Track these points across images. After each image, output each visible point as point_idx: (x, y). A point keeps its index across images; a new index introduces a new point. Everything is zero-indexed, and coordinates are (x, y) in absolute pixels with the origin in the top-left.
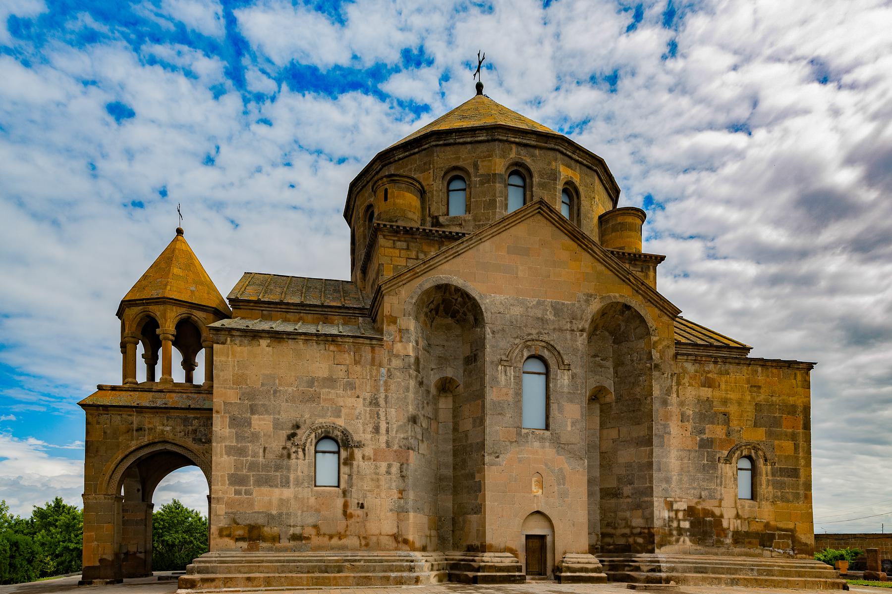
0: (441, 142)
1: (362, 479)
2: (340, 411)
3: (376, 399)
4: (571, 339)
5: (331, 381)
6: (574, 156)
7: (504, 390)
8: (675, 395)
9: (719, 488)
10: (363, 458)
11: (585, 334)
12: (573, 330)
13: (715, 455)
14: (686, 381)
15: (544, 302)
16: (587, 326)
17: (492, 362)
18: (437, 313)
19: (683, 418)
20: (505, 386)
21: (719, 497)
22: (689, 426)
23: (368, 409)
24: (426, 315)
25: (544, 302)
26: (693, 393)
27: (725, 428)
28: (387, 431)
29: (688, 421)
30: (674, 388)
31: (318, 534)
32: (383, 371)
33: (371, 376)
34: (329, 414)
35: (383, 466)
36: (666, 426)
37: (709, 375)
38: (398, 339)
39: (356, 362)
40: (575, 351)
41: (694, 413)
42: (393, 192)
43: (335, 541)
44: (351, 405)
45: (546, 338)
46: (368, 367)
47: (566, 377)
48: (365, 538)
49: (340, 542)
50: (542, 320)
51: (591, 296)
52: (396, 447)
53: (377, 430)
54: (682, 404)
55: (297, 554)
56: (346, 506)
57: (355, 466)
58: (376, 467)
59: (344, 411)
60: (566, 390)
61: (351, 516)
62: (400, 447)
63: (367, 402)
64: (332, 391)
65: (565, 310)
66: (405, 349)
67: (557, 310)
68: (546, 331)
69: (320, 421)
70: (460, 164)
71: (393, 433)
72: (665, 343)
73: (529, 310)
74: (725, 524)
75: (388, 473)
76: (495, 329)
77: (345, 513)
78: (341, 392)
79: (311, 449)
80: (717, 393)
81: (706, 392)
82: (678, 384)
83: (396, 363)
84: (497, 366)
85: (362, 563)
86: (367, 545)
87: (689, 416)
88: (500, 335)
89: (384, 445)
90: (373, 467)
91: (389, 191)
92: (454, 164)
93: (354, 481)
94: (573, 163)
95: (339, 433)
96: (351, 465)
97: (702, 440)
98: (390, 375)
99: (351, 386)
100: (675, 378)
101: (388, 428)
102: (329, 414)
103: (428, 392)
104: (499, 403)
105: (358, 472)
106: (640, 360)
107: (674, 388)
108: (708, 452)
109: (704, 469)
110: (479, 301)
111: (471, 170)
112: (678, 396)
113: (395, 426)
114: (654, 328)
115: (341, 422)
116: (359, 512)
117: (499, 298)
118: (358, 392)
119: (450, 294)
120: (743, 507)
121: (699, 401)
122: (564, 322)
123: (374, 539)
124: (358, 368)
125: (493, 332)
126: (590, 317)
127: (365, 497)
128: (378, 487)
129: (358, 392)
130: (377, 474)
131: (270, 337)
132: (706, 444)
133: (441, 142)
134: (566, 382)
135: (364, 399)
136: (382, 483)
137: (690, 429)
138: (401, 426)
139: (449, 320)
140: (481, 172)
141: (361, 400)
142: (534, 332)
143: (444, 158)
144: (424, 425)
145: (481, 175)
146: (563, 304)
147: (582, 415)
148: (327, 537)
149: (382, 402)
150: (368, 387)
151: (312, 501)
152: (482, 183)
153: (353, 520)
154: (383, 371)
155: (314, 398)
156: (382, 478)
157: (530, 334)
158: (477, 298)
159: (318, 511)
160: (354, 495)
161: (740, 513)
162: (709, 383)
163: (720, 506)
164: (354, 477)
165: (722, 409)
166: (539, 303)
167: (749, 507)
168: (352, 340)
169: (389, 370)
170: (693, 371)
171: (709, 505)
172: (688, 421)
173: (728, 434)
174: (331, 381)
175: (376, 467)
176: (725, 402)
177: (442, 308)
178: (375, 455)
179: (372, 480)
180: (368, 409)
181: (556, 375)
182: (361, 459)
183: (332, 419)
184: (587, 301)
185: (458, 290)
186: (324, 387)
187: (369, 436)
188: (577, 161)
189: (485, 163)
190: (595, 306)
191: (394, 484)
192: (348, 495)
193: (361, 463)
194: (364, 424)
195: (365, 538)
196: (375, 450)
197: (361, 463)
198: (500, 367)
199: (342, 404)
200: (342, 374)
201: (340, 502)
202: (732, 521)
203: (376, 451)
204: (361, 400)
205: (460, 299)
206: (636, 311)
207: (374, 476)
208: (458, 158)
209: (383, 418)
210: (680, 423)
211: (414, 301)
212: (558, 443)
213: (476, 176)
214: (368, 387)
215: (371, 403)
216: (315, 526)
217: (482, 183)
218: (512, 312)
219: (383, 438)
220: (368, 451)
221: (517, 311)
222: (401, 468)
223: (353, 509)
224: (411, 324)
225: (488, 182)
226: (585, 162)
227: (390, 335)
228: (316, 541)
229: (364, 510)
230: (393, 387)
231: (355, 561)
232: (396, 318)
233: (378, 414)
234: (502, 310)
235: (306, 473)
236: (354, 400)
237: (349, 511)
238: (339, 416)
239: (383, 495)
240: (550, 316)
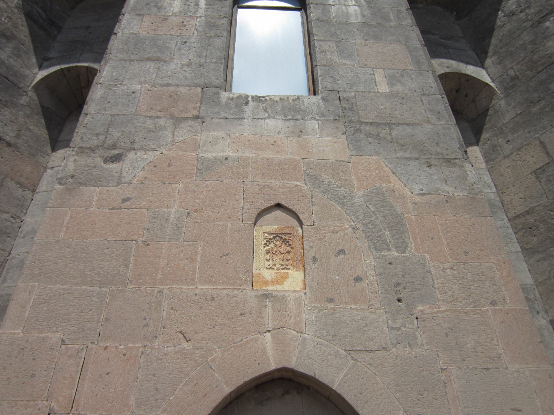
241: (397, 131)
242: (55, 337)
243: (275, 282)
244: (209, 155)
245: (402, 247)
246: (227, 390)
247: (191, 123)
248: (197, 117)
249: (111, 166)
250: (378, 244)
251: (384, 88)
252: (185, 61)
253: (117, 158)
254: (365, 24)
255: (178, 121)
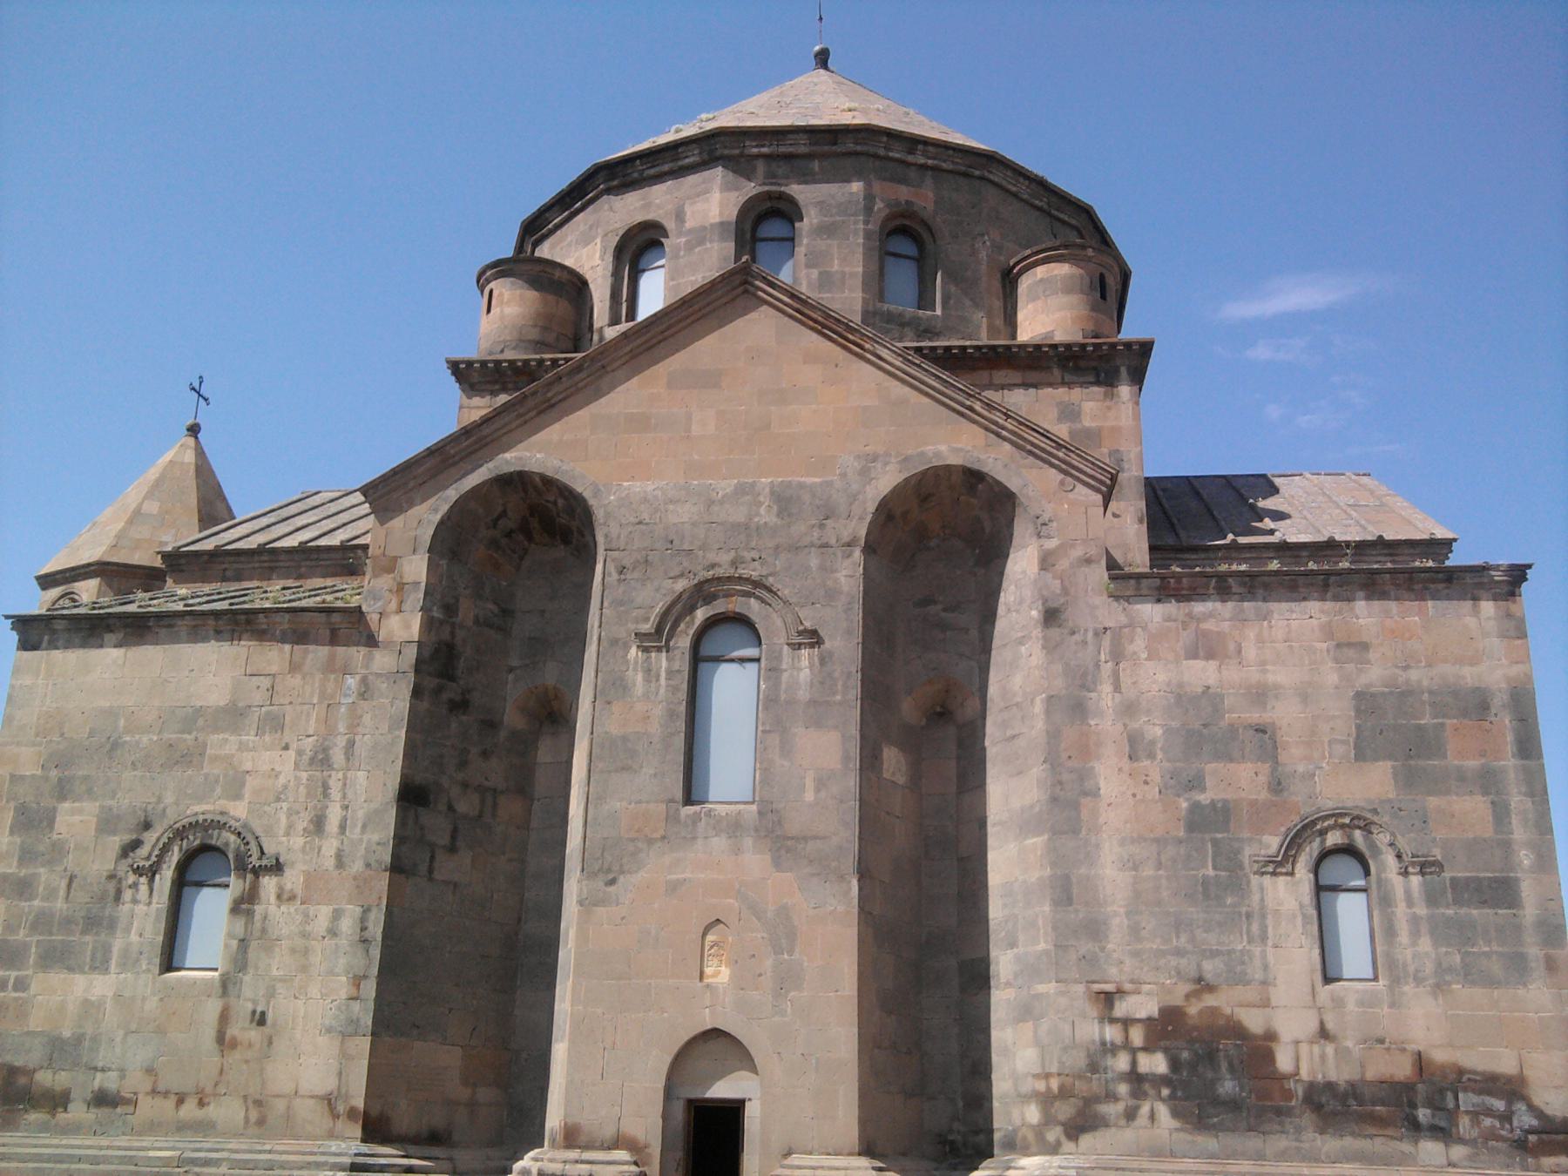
0: (615, 183)
1: (269, 950)
2: (243, 784)
3: (325, 750)
4: (822, 568)
5: (233, 716)
6: (910, 158)
7: (640, 707)
8: (1106, 688)
9: (1257, 950)
10: (279, 897)
11: (857, 554)
12: (826, 546)
13: (1238, 852)
14: (1138, 645)
15: (753, 485)
16: (863, 533)
17: (614, 642)
18: (530, 538)
19: (1136, 748)
20: (646, 696)
21: (1259, 976)
22: (1155, 770)
23: (304, 775)
24: (494, 544)
25: (753, 485)
26: (1162, 677)
27: (1265, 768)
28: (343, 827)
29: (1151, 756)
30: (1107, 668)
31: (154, 1092)
32: (351, 682)
33: (323, 695)
34: (219, 790)
35: (324, 912)
36: (1084, 775)
37: (1204, 626)
38: (393, 605)
39: (294, 667)
40: (831, 595)
41: (1168, 731)
42: (501, 295)
43: (189, 1110)
44: (266, 767)
45: (753, 571)
46: (319, 676)
47: (805, 663)
48: (259, 1103)
49: (200, 1114)
50: (746, 529)
51: (875, 459)
52: (357, 866)
53: (319, 824)
54: (1129, 709)
55: (104, 1142)
56: (224, 1018)
57: (257, 917)
58: (307, 918)
59: (251, 783)
60: (803, 694)
61: (234, 1044)
62: (368, 865)
63: (306, 758)
64: (232, 738)
65: (807, 498)
66: (408, 627)
67: (785, 501)
68: (755, 555)
69: (201, 809)
70: (650, 216)
71: (354, 833)
72: (1078, 552)
73: (716, 508)
74: (1284, 1062)
75: (333, 932)
76: (626, 562)
77: (223, 1041)
78: (250, 738)
79: (167, 874)
80: (1232, 674)
81: (1201, 673)
82: (1117, 656)
83: (383, 661)
84: (627, 648)
85: (223, 1169)
86: (261, 1122)
87: (1153, 743)
88: (636, 575)
89: (330, 863)
90: (299, 918)
91: (495, 294)
92: (639, 218)
93: (252, 954)
94: (912, 174)
95: (232, 838)
96: (250, 914)
97: (1195, 807)
98: (365, 692)
99: (275, 723)
100: (1106, 641)
101: (344, 819)
102: (219, 790)
103: (491, 725)
104: (625, 739)
105: (264, 930)
106: (1020, 603)
107: (1107, 668)
108: (1215, 843)
109: (1206, 895)
110: (591, 502)
111: (670, 225)
112: (1117, 688)
113: (360, 814)
114: (1046, 517)
115: (239, 811)
116: (254, 1034)
117: (636, 487)
118: (288, 736)
119: (535, 488)
120: (1338, 1003)
121: (1182, 699)
122: (803, 528)
123: (280, 1105)
124: (296, 681)
125: (622, 570)
126: (871, 507)
127: (271, 994)
128: (304, 969)
129: (286, 739)
130: (305, 935)
131: (126, 626)
132: (1209, 822)
133: (615, 183)
134: (805, 675)
135: (300, 753)
136: (316, 958)
137: (1156, 776)
138: (376, 812)
139: (560, 552)
140: (688, 225)
141: (292, 754)
142: (725, 558)
143: (621, 211)
144: (462, 807)
145: (690, 231)
146: (801, 486)
147: (846, 758)
148: (173, 1099)
149: (338, 756)
150: (312, 722)
151: (152, 1004)
152: (690, 247)
153: (236, 1056)
154: (351, 682)
155: (186, 758)
156: (317, 946)
157: (713, 566)
158: (587, 494)
159: (161, 1031)
160: (247, 992)
161: (1330, 1026)
162: (1207, 648)
163: (1265, 1003)
164: (254, 944)
165: (1255, 716)
166: (741, 490)
167: (1361, 1003)
168: (287, 616)
169: (364, 680)
170: (1157, 618)
171: (1224, 1001)
172: (1151, 756)
173: (1277, 786)
174: (233, 716)
175: (307, 918)
176: (1260, 695)
177: (535, 523)
178: (307, 885)
179: (293, 951)
180: (304, 775)
181: (779, 658)
182: (273, 899)
183: (223, 804)
184: (865, 473)
185: (548, 482)
186: (217, 730)
187: (298, 841)
188: (924, 167)
189: (699, 206)
190: (886, 481)
191: (342, 961)
192: (232, 990)
193: (273, 909)
194: (290, 813)
195: (259, 1103)
196: (307, 874)
197: (273, 909)
198: (633, 650)
199: (248, 766)
200: (258, 697)
201: (213, 1008)
202: (1304, 1048)
203: (309, 877)
204: (292, 754)
205: (561, 502)
206: (999, 483)
207: (299, 942)
208: (647, 206)
209: (335, 793)
210: (1126, 764)
211: (438, 517)
212: (772, 828)
213: (680, 234)
214: (312, 722)
215: (312, 760)
216: (150, 1071)
217: (690, 247)
218: (673, 519)
219: (330, 846)
220: (293, 879)
221: (683, 514)
222: (363, 920)
223: (240, 1029)
224: (416, 568)
225: (701, 242)
226: (944, 165)
227: (375, 599)
228: (148, 1108)
229: (266, 1030)
230: (367, 719)
231: (207, 1163)
232: (395, 559)
233: (326, 787)
234: (646, 516)
235: (148, 935)
236: (276, 754)
237: (233, 1031)
238: (238, 796)
239: (314, 991)
240: (766, 515)
241: (811, 846)
242: (599, 1011)
243: (713, 976)
244: (674, 877)
245: (791, 952)
246: (686, 1039)
247: (659, 844)
248: (663, 838)
249: (611, 889)
250: (778, 951)
251: (809, 796)
252: (652, 771)
253: (612, 882)
254: (813, 702)
255: (650, 842)
